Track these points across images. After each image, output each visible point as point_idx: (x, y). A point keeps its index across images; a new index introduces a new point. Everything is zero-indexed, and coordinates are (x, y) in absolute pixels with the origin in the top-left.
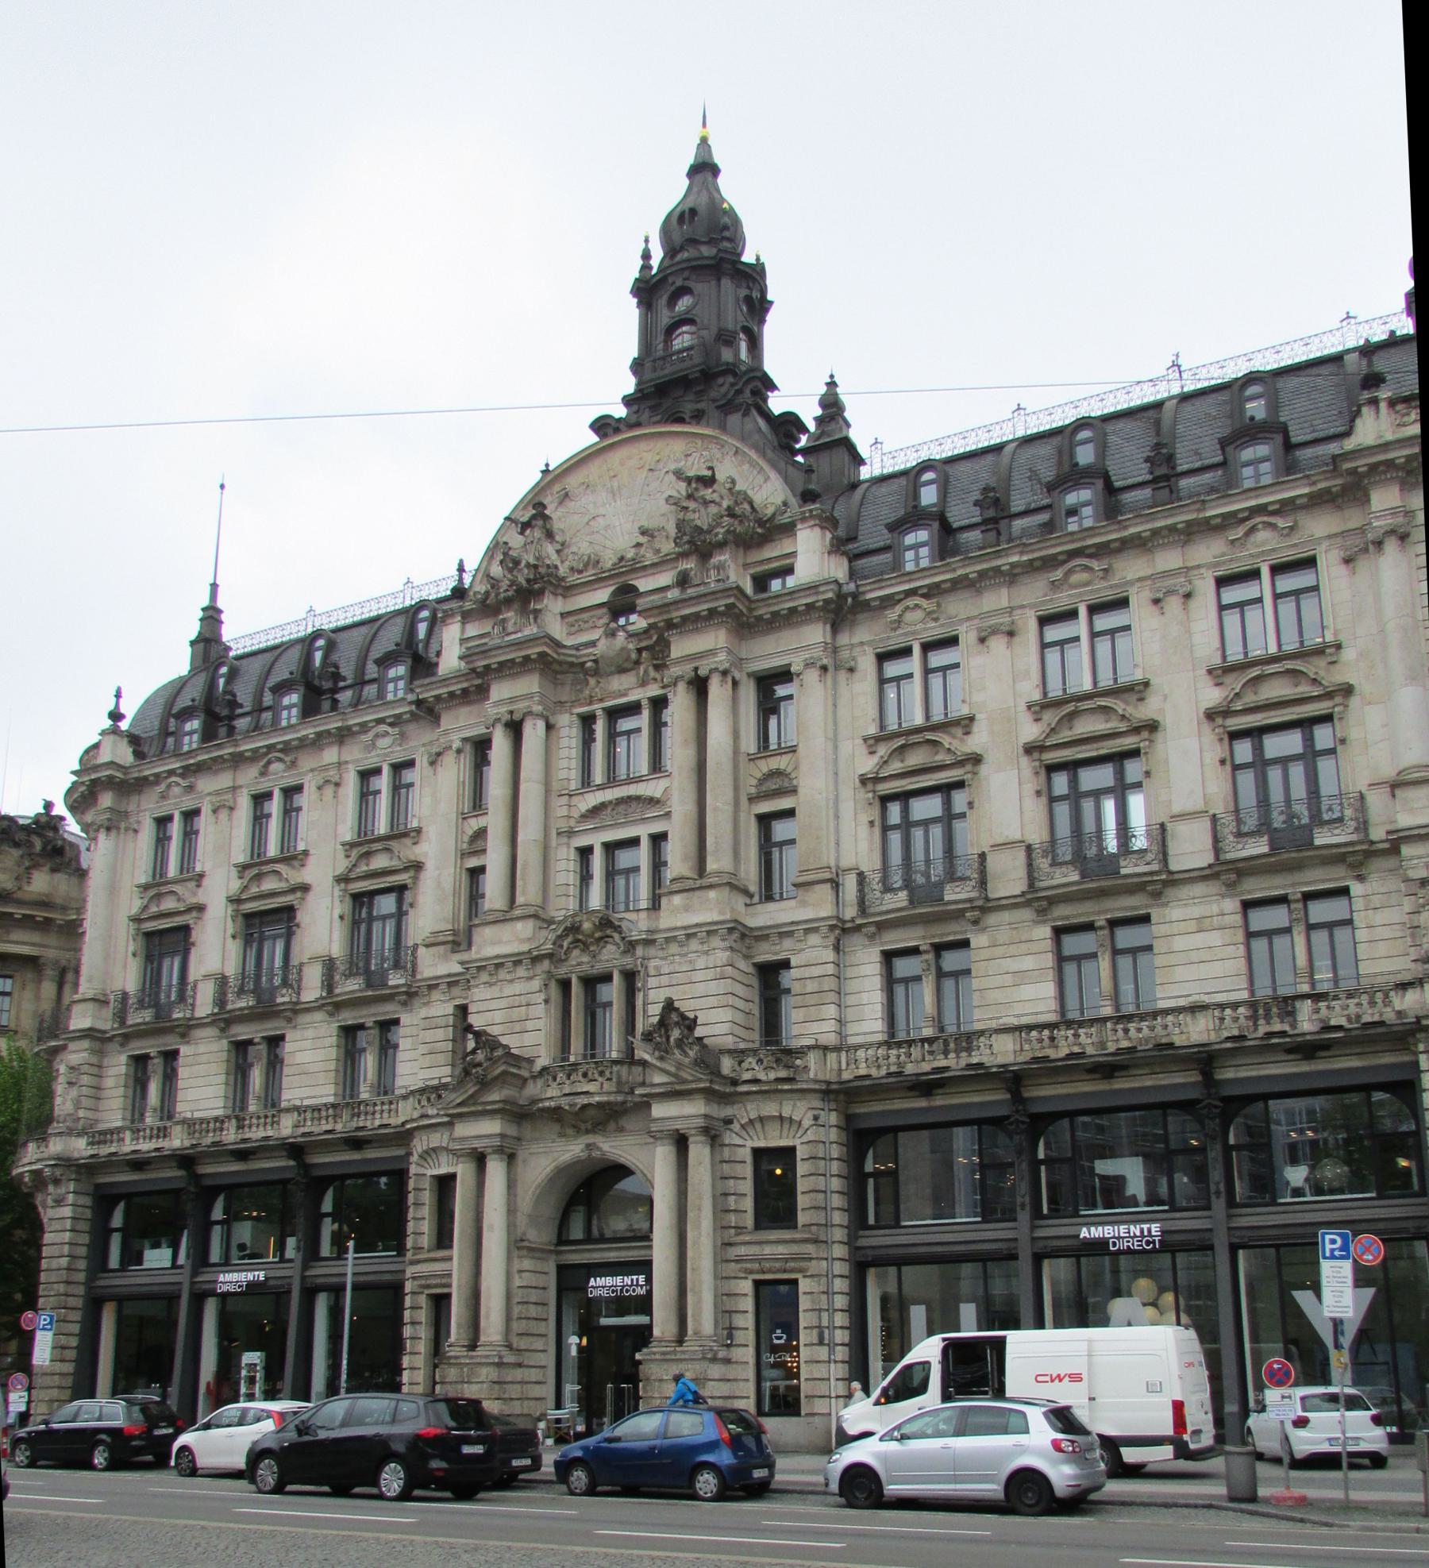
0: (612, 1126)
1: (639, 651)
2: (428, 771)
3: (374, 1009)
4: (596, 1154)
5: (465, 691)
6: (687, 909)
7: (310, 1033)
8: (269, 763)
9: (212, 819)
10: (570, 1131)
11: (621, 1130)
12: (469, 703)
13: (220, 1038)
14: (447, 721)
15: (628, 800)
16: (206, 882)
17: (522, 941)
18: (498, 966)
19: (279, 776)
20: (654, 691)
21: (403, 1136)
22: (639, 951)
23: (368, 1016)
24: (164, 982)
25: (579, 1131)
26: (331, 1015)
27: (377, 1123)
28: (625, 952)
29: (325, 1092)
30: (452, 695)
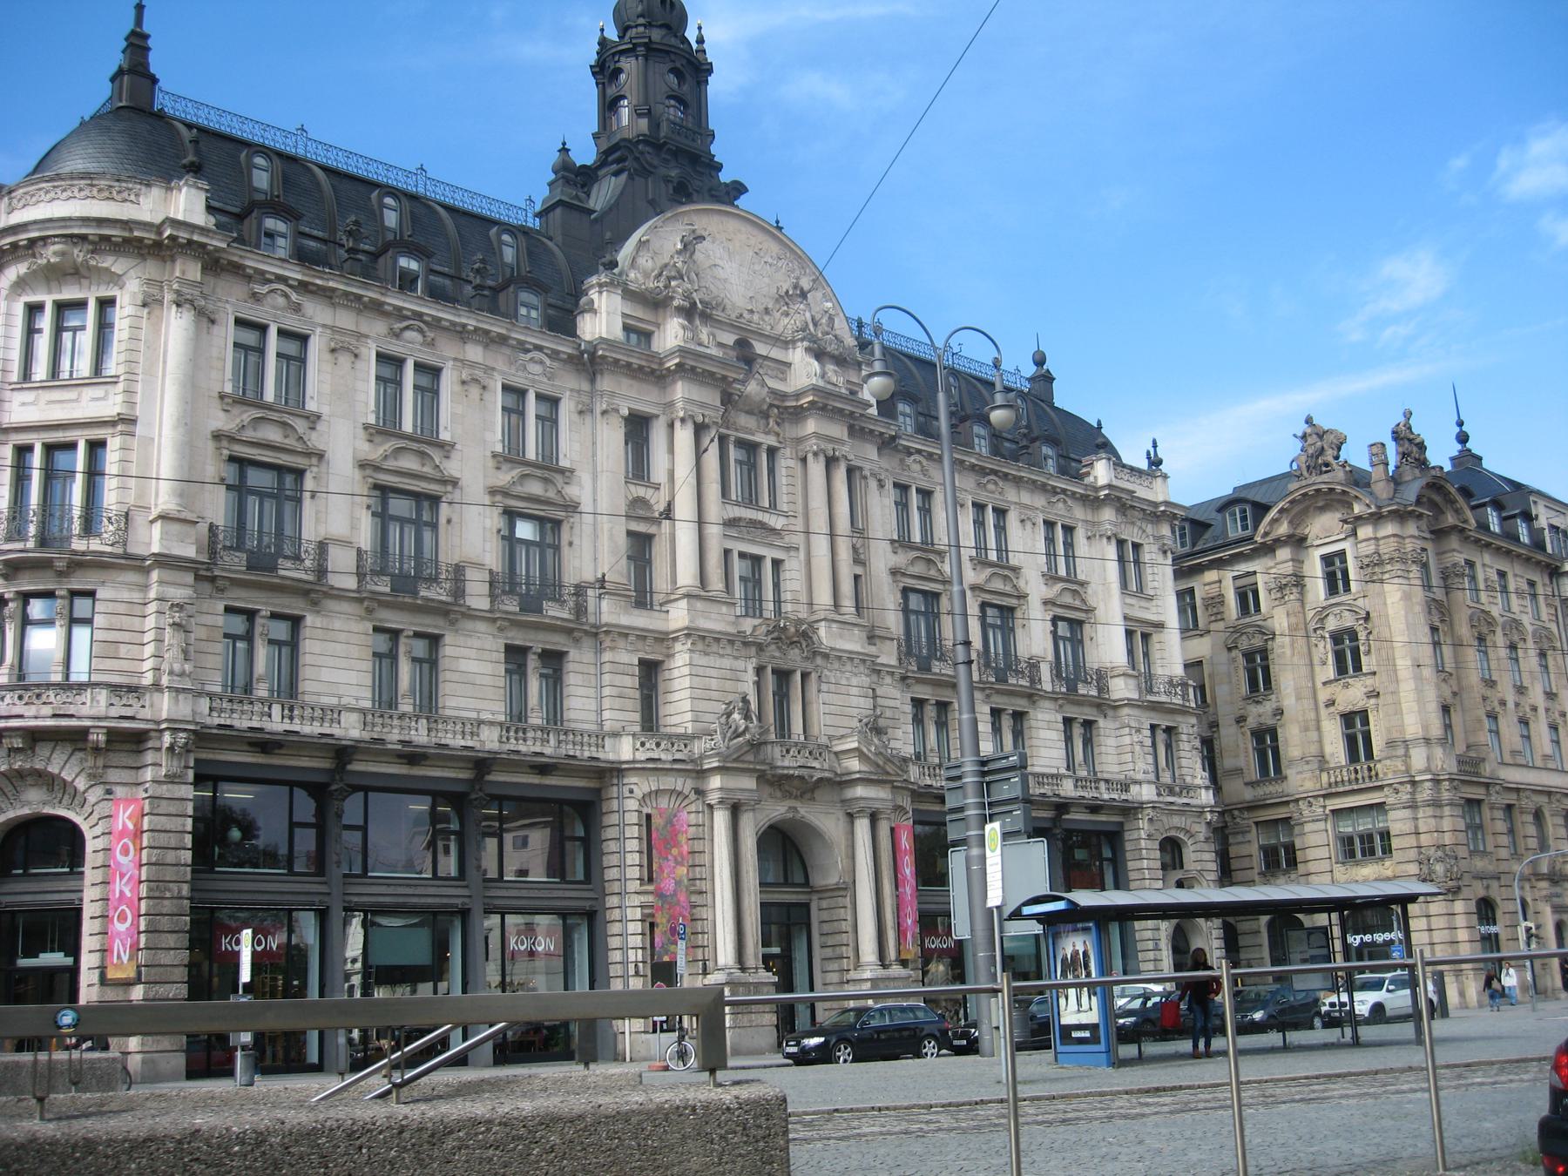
0: (808, 795)
1: (771, 405)
2: (575, 417)
3: (542, 636)
4: (798, 816)
5: (641, 368)
6: (841, 636)
7: (477, 643)
8: (407, 328)
9: (328, 356)
10: (779, 794)
11: (813, 799)
12: (634, 378)
13: (363, 619)
14: (606, 383)
15: (754, 524)
16: (320, 427)
17: (729, 623)
18: (717, 640)
19: (411, 347)
20: (771, 441)
21: (616, 771)
22: (819, 661)
23: (538, 642)
24: (249, 526)
25: (788, 795)
26: (501, 629)
27: (587, 754)
28: (807, 658)
29: (495, 708)
30: (629, 365)
